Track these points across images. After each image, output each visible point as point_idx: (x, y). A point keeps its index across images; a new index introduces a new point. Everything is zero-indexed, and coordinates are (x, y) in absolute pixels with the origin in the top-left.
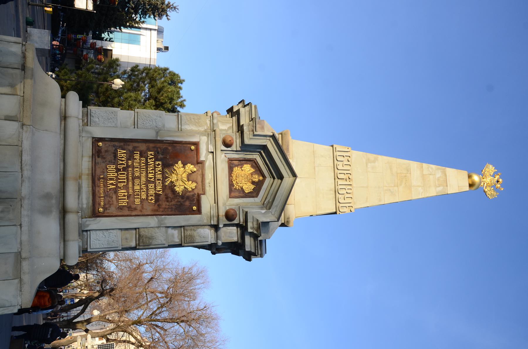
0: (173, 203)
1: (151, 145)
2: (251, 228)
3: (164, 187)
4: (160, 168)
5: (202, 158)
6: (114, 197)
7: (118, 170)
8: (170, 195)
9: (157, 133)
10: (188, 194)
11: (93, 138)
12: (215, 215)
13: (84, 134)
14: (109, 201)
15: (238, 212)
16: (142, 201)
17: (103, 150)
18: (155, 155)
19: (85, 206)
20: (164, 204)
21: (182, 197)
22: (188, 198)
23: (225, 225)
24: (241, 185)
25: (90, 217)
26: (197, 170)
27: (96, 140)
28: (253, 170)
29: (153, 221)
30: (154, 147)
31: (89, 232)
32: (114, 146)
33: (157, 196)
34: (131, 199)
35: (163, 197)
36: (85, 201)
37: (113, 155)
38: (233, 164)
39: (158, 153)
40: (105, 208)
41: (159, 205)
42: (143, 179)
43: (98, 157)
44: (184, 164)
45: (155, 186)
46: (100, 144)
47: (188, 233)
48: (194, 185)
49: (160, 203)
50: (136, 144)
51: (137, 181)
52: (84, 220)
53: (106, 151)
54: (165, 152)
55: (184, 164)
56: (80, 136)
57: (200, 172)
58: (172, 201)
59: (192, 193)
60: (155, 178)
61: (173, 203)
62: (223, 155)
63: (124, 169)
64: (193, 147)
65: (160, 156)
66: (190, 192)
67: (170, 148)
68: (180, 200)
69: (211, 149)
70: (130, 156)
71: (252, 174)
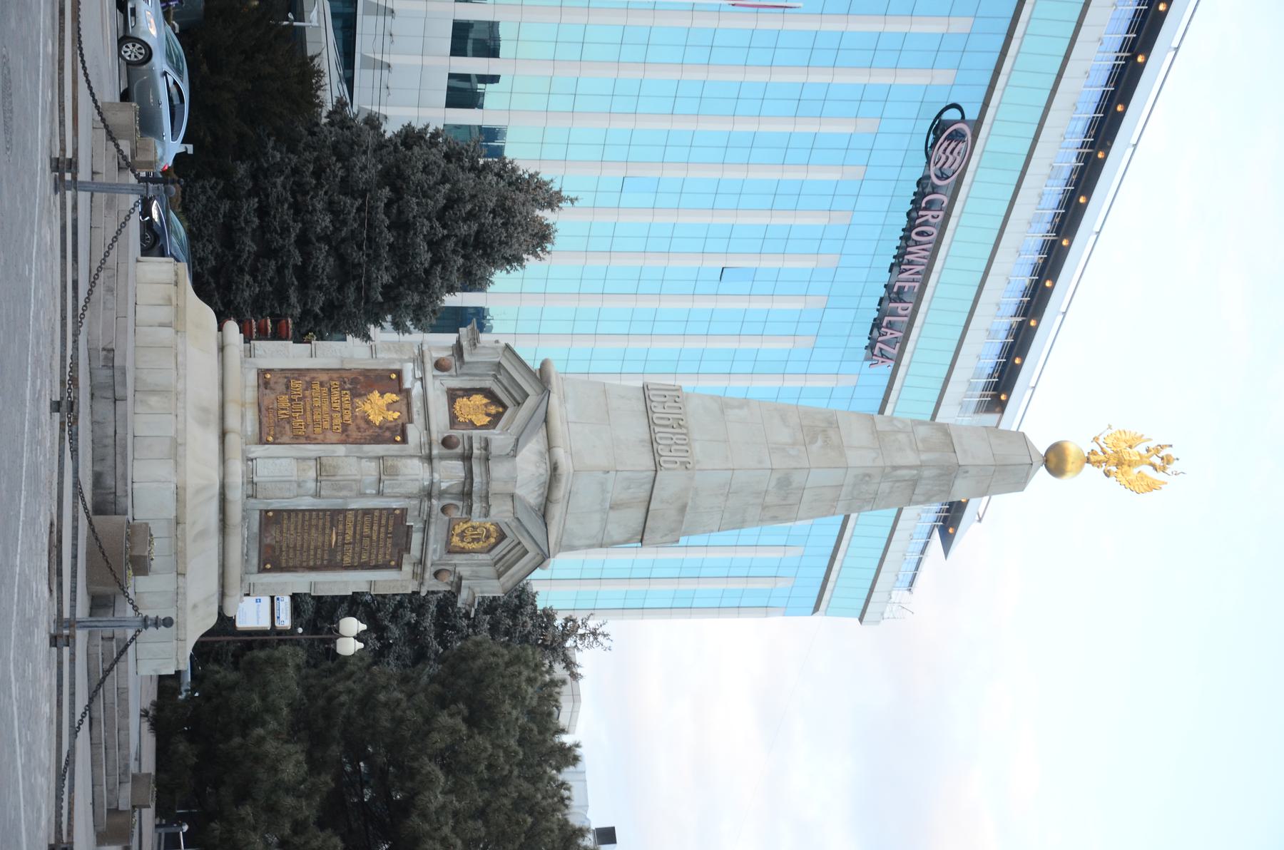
0: (367, 433)
1: (335, 375)
2: (478, 449)
3: (354, 418)
4: (348, 397)
5: (407, 385)
6: (287, 427)
7: (292, 400)
8: (363, 425)
9: (342, 361)
10: (388, 424)
11: (258, 369)
12: (426, 442)
13: (247, 366)
14: (281, 431)
15: (461, 440)
16: (324, 430)
17: (271, 382)
18: (340, 385)
19: (249, 433)
20: (355, 434)
21: (380, 427)
22: (388, 428)
23: (442, 458)
24: (469, 417)
25: (256, 444)
26: (401, 400)
27: (262, 373)
28: (485, 401)
29: (341, 450)
30: (338, 378)
31: (254, 461)
32: (286, 377)
33: (345, 427)
34: (310, 428)
35: (352, 427)
36: (249, 429)
37: (284, 387)
38: (455, 395)
39: (345, 383)
40: (275, 438)
41: (347, 436)
42: (325, 408)
43: (266, 388)
44: (382, 394)
45: (342, 416)
46: (268, 376)
47: (390, 462)
48: (396, 415)
49: (349, 433)
50: (315, 375)
51: (317, 411)
52: (248, 446)
53: (276, 383)
54: (354, 381)
55: (382, 394)
56: (242, 367)
57: (405, 402)
58: (365, 432)
59: (394, 424)
60: (341, 408)
61: (367, 433)
62: (437, 382)
63: (299, 399)
64: (394, 376)
65: (348, 386)
66: (391, 421)
67: (361, 378)
68: (377, 430)
69: (419, 374)
70: (307, 387)
71: (486, 405)
